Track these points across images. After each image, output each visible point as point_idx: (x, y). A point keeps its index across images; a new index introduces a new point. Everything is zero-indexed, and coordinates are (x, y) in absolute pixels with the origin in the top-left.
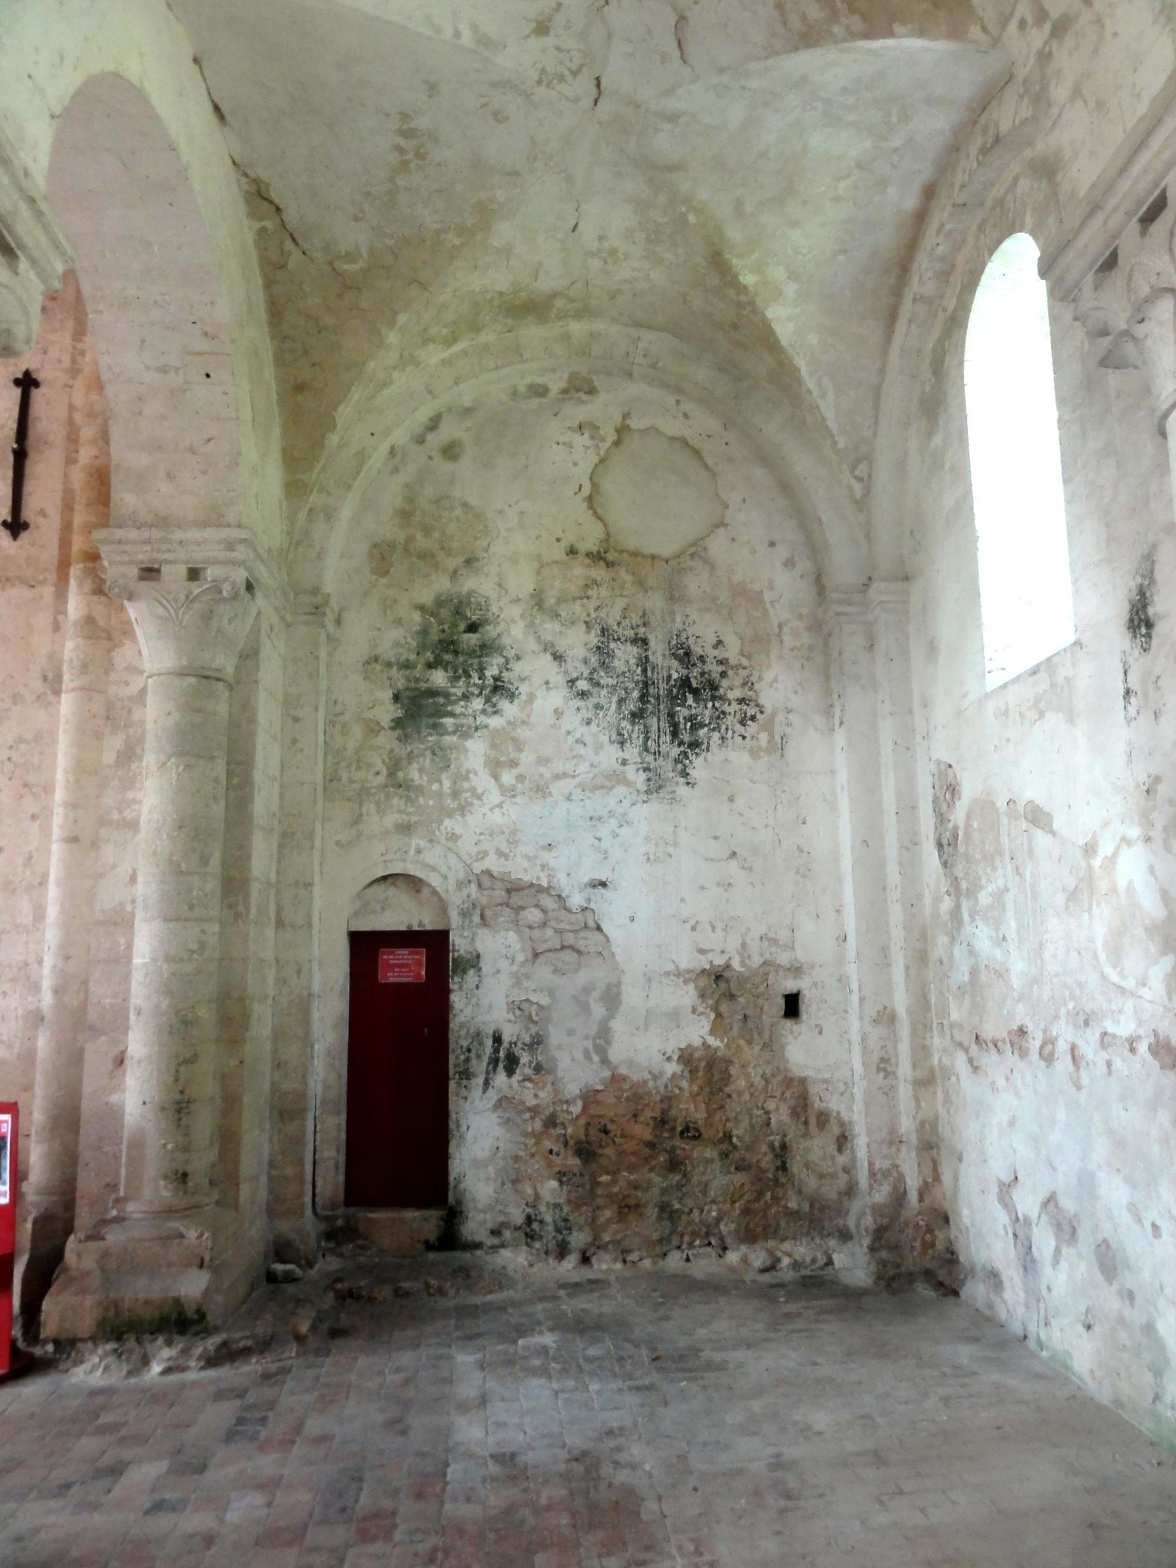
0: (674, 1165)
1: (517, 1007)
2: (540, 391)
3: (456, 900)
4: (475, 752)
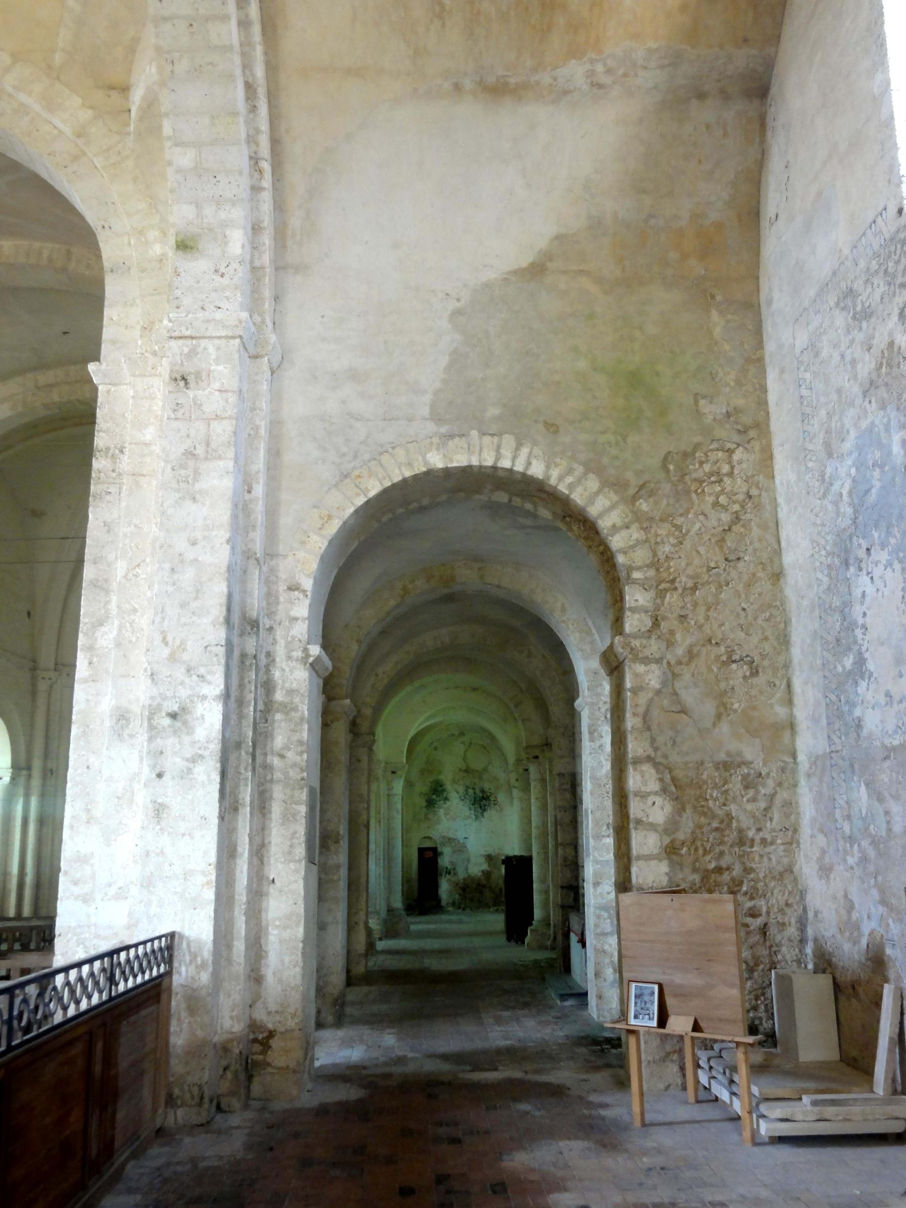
0: (481, 892)
1: (451, 862)
2: (453, 735)
3: (438, 841)
4: (441, 812)
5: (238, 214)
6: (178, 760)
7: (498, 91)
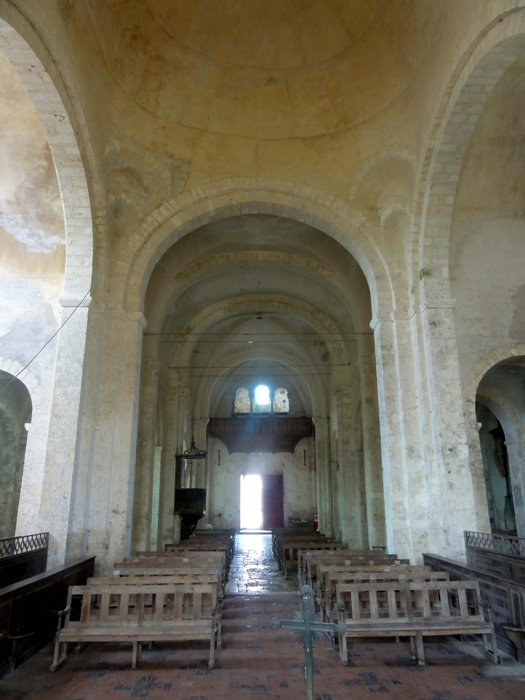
5: (446, 262)
6: (455, 467)
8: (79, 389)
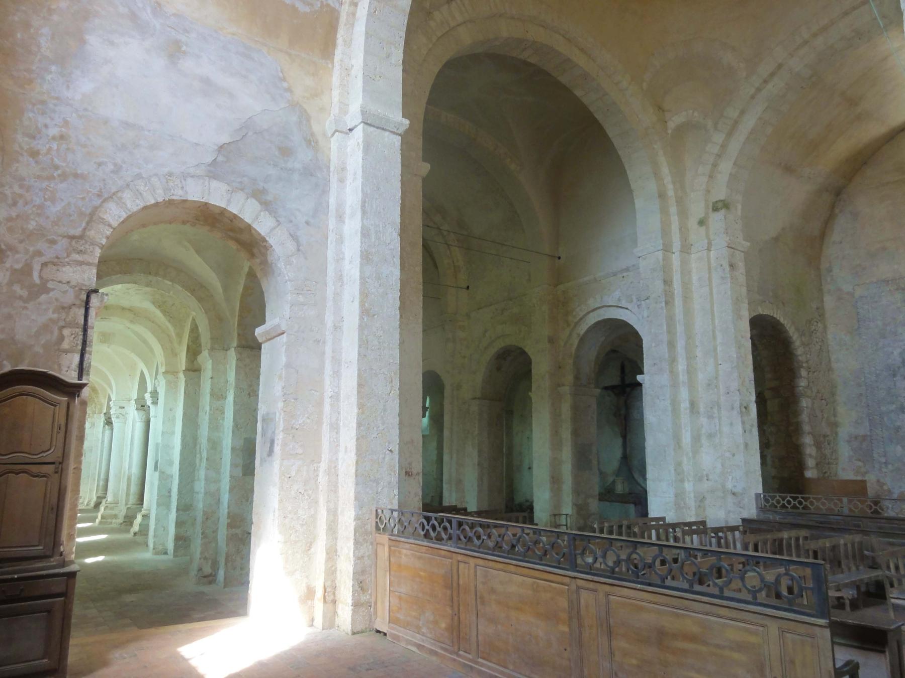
7: (788, 169)
8: (397, 272)
